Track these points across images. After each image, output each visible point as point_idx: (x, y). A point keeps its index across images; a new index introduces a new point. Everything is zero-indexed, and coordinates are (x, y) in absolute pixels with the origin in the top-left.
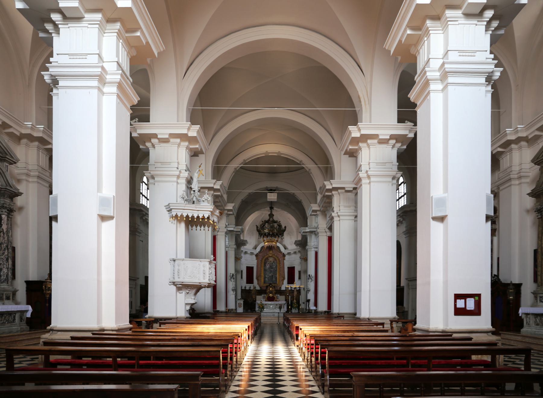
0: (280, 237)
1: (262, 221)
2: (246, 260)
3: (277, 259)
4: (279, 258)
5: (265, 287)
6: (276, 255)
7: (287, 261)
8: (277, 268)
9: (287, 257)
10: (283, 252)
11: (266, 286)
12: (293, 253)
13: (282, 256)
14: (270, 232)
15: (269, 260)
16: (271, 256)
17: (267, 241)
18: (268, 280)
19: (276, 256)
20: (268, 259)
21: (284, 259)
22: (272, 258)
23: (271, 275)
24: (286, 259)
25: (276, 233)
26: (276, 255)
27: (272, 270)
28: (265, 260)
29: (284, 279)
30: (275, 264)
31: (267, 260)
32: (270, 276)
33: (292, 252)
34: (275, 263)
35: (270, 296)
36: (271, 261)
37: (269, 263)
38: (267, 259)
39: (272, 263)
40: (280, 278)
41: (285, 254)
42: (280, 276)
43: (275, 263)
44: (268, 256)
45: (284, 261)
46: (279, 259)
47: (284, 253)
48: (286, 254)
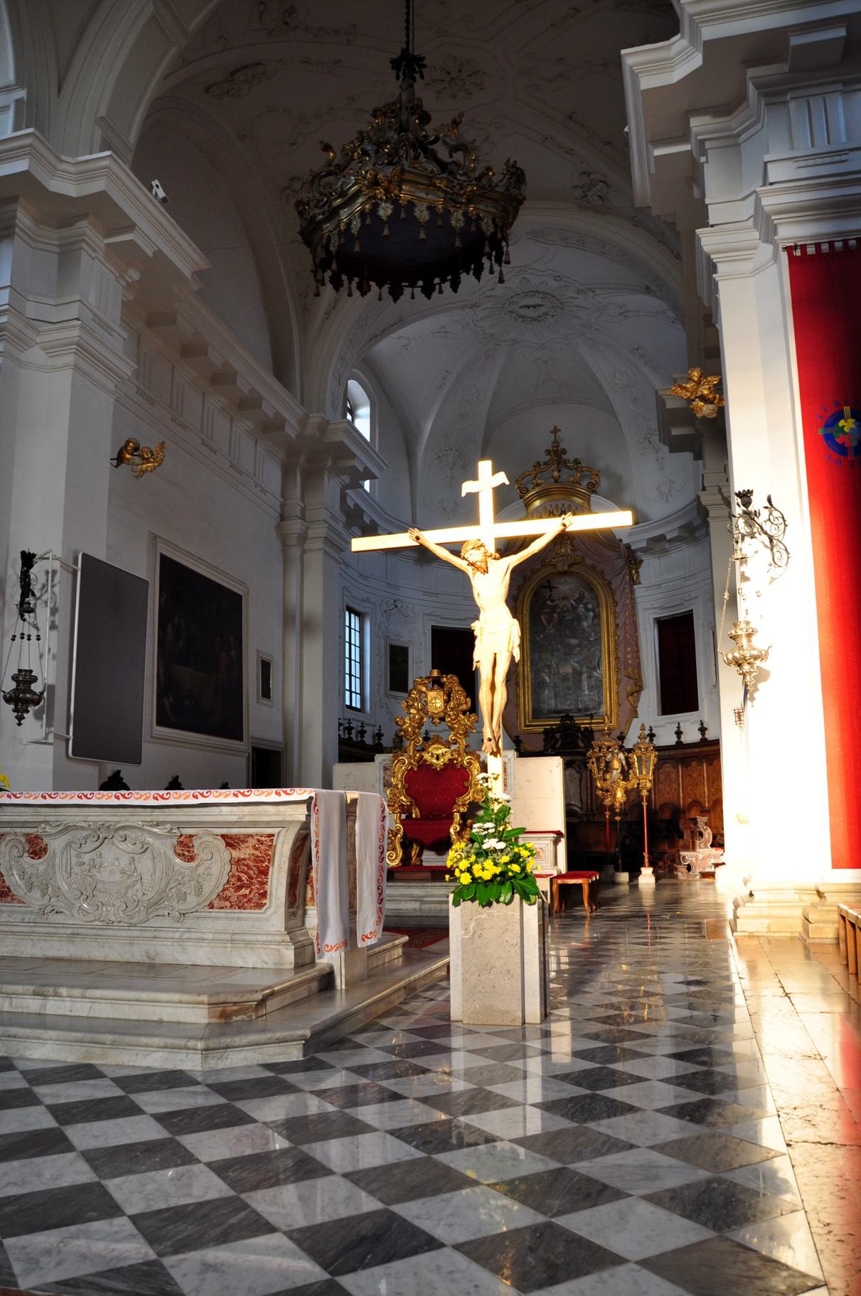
0: (485, 273)
1: (327, 148)
2: (425, 593)
3: (596, 582)
4: (607, 578)
5: (543, 737)
6: (588, 562)
7: (647, 588)
8: (598, 633)
9: (650, 569)
10: (625, 542)
11: (541, 729)
12: (676, 534)
13: (621, 562)
14: (375, 207)
15: (554, 592)
16: (566, 568)
17: (537, 489)
18: (556, 695)
19: (593, 568)
20: (551, 588)
21: (634, 582)
22: (569, 580)
23: (569, 670)
24: (641, 579)
25: (431, 209)
26: (588, 562)
27: (574, 641)
28: (536, 594)
29: (638, 688)
30: (587, 610)
31: (547, 592)
32: (565, 678)
33: (671, 531)
34: (585, 605)
35: (424, 766)
36: (565, 598)
37: (556, 606)
38: (543, 587)
39: (575, 608)
40: (618, 682)
41: (633, 548)
42: (618, 671)
43: (585, 605)
44: (551, 570)
45: (632, 592)
46: (609, 583)
47: (628, 547)
48: (644, 550)
